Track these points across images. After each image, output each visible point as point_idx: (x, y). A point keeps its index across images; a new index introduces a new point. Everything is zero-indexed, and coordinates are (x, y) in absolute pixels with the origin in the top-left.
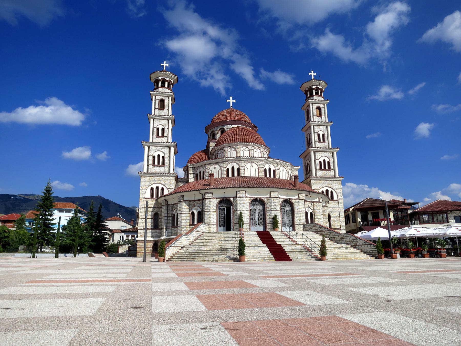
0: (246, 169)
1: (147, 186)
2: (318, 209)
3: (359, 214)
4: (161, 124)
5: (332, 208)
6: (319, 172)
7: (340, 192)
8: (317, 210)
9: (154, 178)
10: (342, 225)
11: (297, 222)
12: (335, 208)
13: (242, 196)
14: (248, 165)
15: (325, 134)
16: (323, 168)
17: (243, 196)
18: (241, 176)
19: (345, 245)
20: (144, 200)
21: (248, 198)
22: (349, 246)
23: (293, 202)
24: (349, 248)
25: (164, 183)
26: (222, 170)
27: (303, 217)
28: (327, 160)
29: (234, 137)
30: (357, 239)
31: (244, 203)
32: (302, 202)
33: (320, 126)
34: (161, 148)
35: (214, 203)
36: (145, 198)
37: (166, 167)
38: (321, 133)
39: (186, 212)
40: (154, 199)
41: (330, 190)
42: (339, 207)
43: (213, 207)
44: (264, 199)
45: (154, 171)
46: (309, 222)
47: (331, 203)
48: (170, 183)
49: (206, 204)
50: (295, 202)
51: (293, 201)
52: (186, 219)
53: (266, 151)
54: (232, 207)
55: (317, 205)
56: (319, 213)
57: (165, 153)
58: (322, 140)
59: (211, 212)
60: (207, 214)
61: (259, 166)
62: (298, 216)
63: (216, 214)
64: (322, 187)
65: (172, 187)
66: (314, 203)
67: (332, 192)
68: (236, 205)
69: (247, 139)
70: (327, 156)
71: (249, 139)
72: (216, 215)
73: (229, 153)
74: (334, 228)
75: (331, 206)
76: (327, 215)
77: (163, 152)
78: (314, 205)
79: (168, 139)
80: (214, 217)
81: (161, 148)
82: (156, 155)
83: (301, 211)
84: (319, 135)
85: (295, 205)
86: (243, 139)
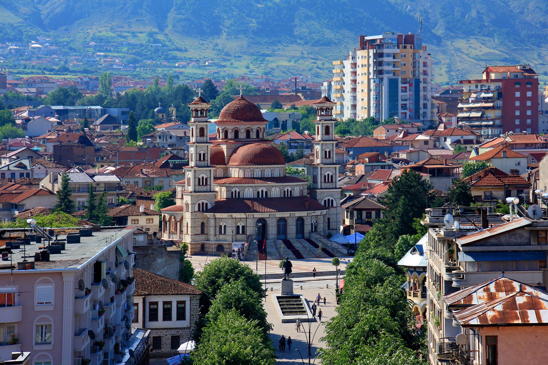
0: (272, 192)
28: (331, 174)
36: (195, 212)
37: (209, 186)
40: (201, 212)
47: (332, 209)
67: (332, 201)
78: (317, 217)
82: (201, 177)
84: (326, 152)
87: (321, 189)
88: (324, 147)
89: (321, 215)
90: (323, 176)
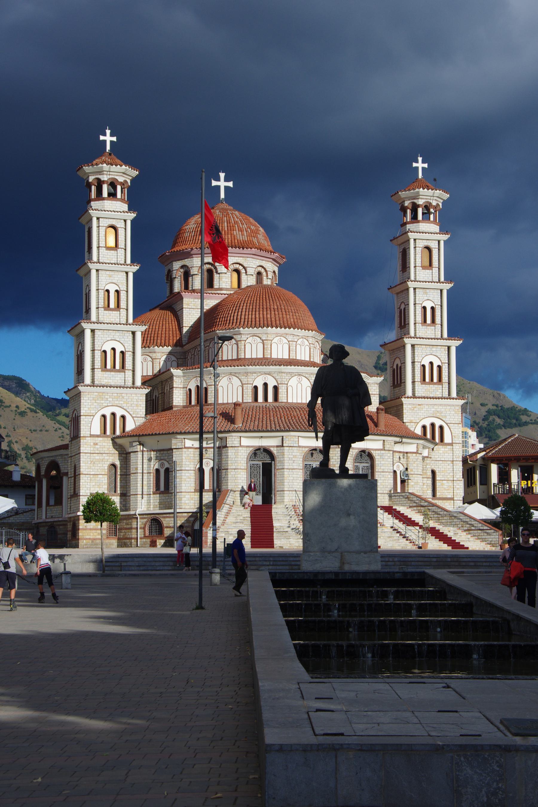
0: (290, 389)
1: (94, 412)
2: (415, 465)
3: (494, 468)
4: (114, 281)
5: (439, 459)
6: (420, 388)
7: (458, 428)
8: (413, 468)
9: (106, 397)
10: (458, 491)
12: (446, 460)
13: (292, 445)
14: (293, 381)
15: (437, 306)
16: (427, 379)
17: (295, 445)
18: (280, 401)
19: (455, 529)
20: (89, 438)
21: (301, 449)
22: (460, 531)
23: (374, 455)
24: (459, 534)
25: (125, 405)
26: (244, 388)
27: (390, 481)
29: (259, 314)
30: (472, 520)
31: (295, 456)
32: (389, 455)
33: (428, 291)
34: (118, 334)
35: (244, 454)
36: (92, 436)
38: (429, 305)
39: (189, 469)
40: (108, 437)
41: (438, 423)
42: (454, 457)
43: (242, 462)
45: (105, 381)
46: (399, 490)
47: (440, 450)
48: (137, 405)
49: (229, 457)
50: (377, 455)
51: (374, 453)
52: (189, 480)
53: (317, 342)
54: (273, 462)
55: (413, 457)
57: (126, 345)
58: (429, 320)
59: (239, 470)
60: (232, 473)
62: (382, 479)
63: (246, 473)
65: (141, 413)
66: (409, 455)
67: (441, 428)
68: (282, 459)
69: (285, 320)
70: (437, 354)
71: (289, 319)
72: (246, 476)
73: (248, 347)
74: (440, 497)
75: (439, 454)
76: (430, 474)
77: (121, 343)
79: (127, 312)
80: (243, 479)
81: (117, 335)
82: (108, 347)
83: (386, 471)
85: (377, 460)
86: (277, 319)
87: (414, 396)
89: (417, 453)
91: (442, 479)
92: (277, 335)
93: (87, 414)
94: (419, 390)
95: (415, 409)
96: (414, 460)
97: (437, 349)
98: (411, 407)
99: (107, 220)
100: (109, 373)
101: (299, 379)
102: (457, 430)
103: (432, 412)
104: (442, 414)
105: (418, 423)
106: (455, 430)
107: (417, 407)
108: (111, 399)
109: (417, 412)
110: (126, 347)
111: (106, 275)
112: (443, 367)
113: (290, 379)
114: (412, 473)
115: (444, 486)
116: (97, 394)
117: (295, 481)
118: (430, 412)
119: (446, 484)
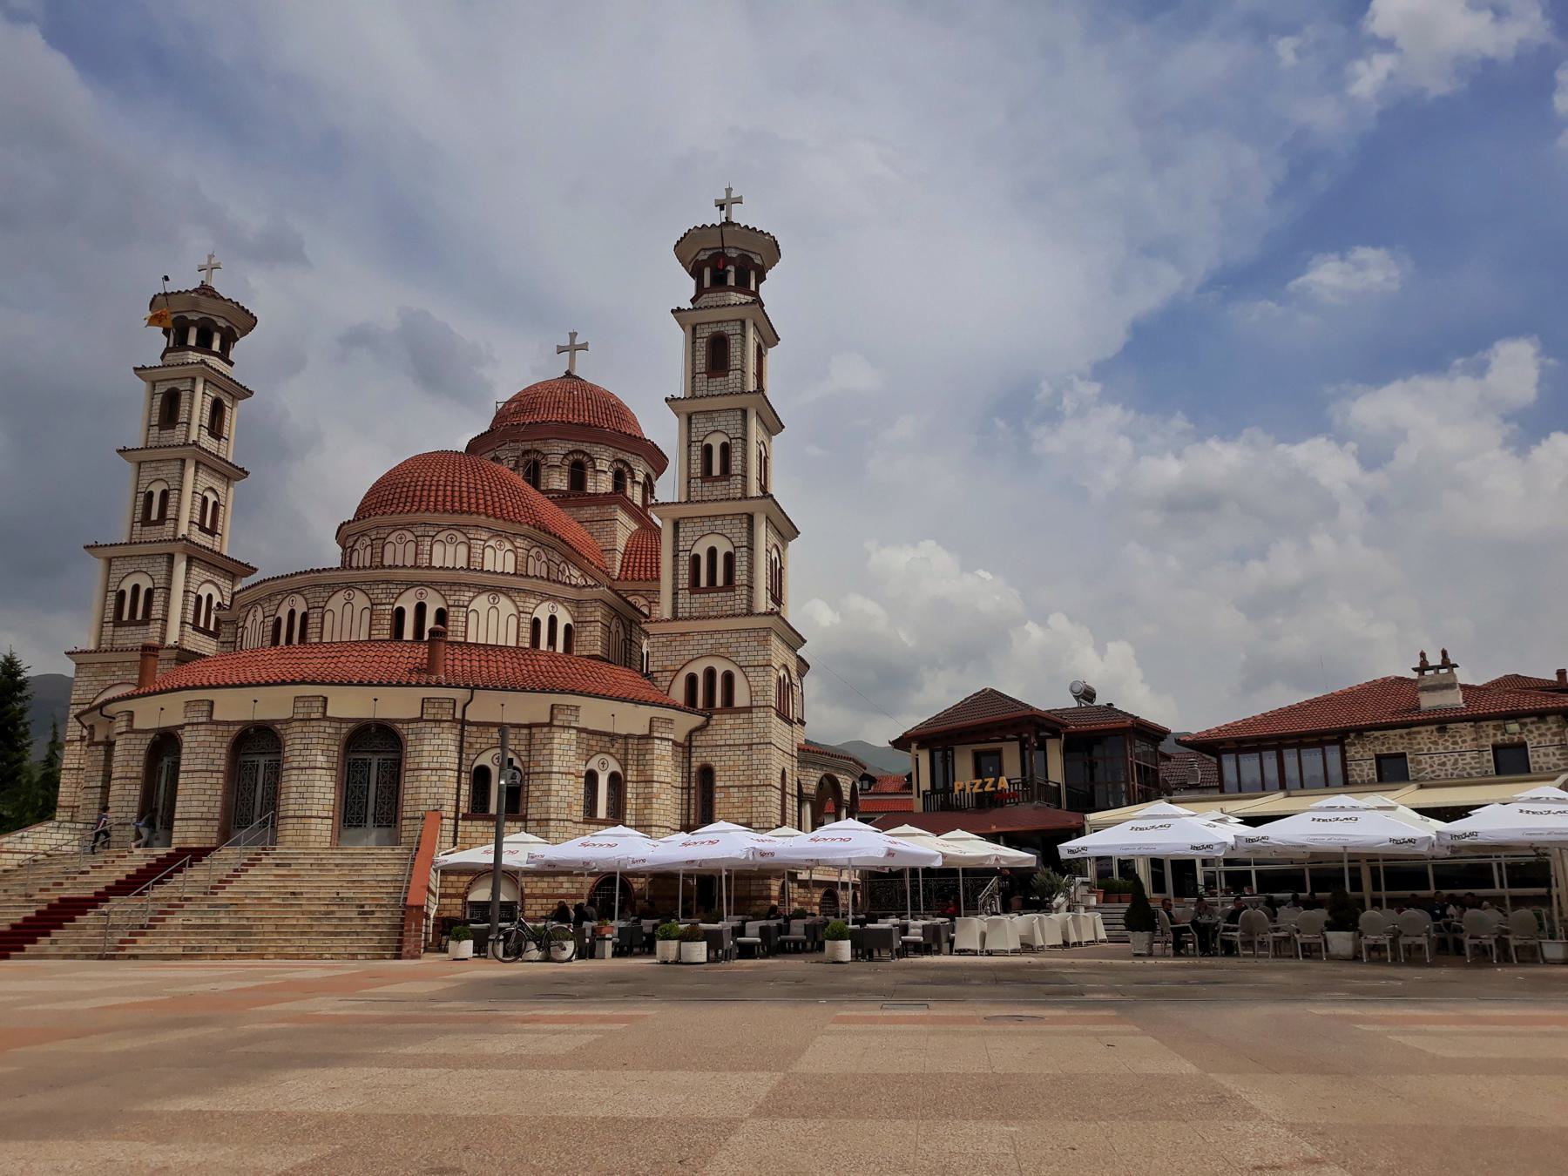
0: (328, 616)
5: (722, 742)
10: (760, 809)
11: (408, 809)
16: (703, 582)
17: (200, 720)
21: (220, 728)
28: (723, 547)
41: (721, 667)
44: (278, 727)
56: (546, 769)
61: (376, 601)
64: (691, 657)
66: (534, 730)
67: (728, 677)
70: (724, 531)
72: (138, 793)
75: (723, 732)
88: (700, 425)
90: (684, 559)
91: (728, 784)
92: (396, 527)
93: (79, 701)
94: (685, 605)
95: (673, 644)
96: (545, 741)
97: (725, 522)
98: (665, 640)
99: (165, 383)
100: (127, 628)
101: (349, 594)
102: (762, 679)
103: (709, 646)
104: (730, 650)
105: (678, 671)
106: (757, 679)
107: (678, 639)
108: (120, 673)
109: (678, 648)
110: (156, 581)
111: (150, 469)
112: (737, 555)
113: (330, 597)
114: (538, 769)
115: (732, 800)
116: (99, 665)
117: (193, 798)
118: (704, 647)
119: (736, 795)
